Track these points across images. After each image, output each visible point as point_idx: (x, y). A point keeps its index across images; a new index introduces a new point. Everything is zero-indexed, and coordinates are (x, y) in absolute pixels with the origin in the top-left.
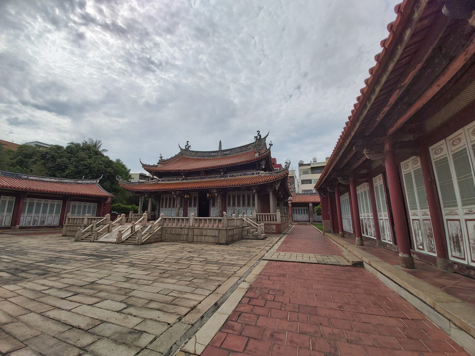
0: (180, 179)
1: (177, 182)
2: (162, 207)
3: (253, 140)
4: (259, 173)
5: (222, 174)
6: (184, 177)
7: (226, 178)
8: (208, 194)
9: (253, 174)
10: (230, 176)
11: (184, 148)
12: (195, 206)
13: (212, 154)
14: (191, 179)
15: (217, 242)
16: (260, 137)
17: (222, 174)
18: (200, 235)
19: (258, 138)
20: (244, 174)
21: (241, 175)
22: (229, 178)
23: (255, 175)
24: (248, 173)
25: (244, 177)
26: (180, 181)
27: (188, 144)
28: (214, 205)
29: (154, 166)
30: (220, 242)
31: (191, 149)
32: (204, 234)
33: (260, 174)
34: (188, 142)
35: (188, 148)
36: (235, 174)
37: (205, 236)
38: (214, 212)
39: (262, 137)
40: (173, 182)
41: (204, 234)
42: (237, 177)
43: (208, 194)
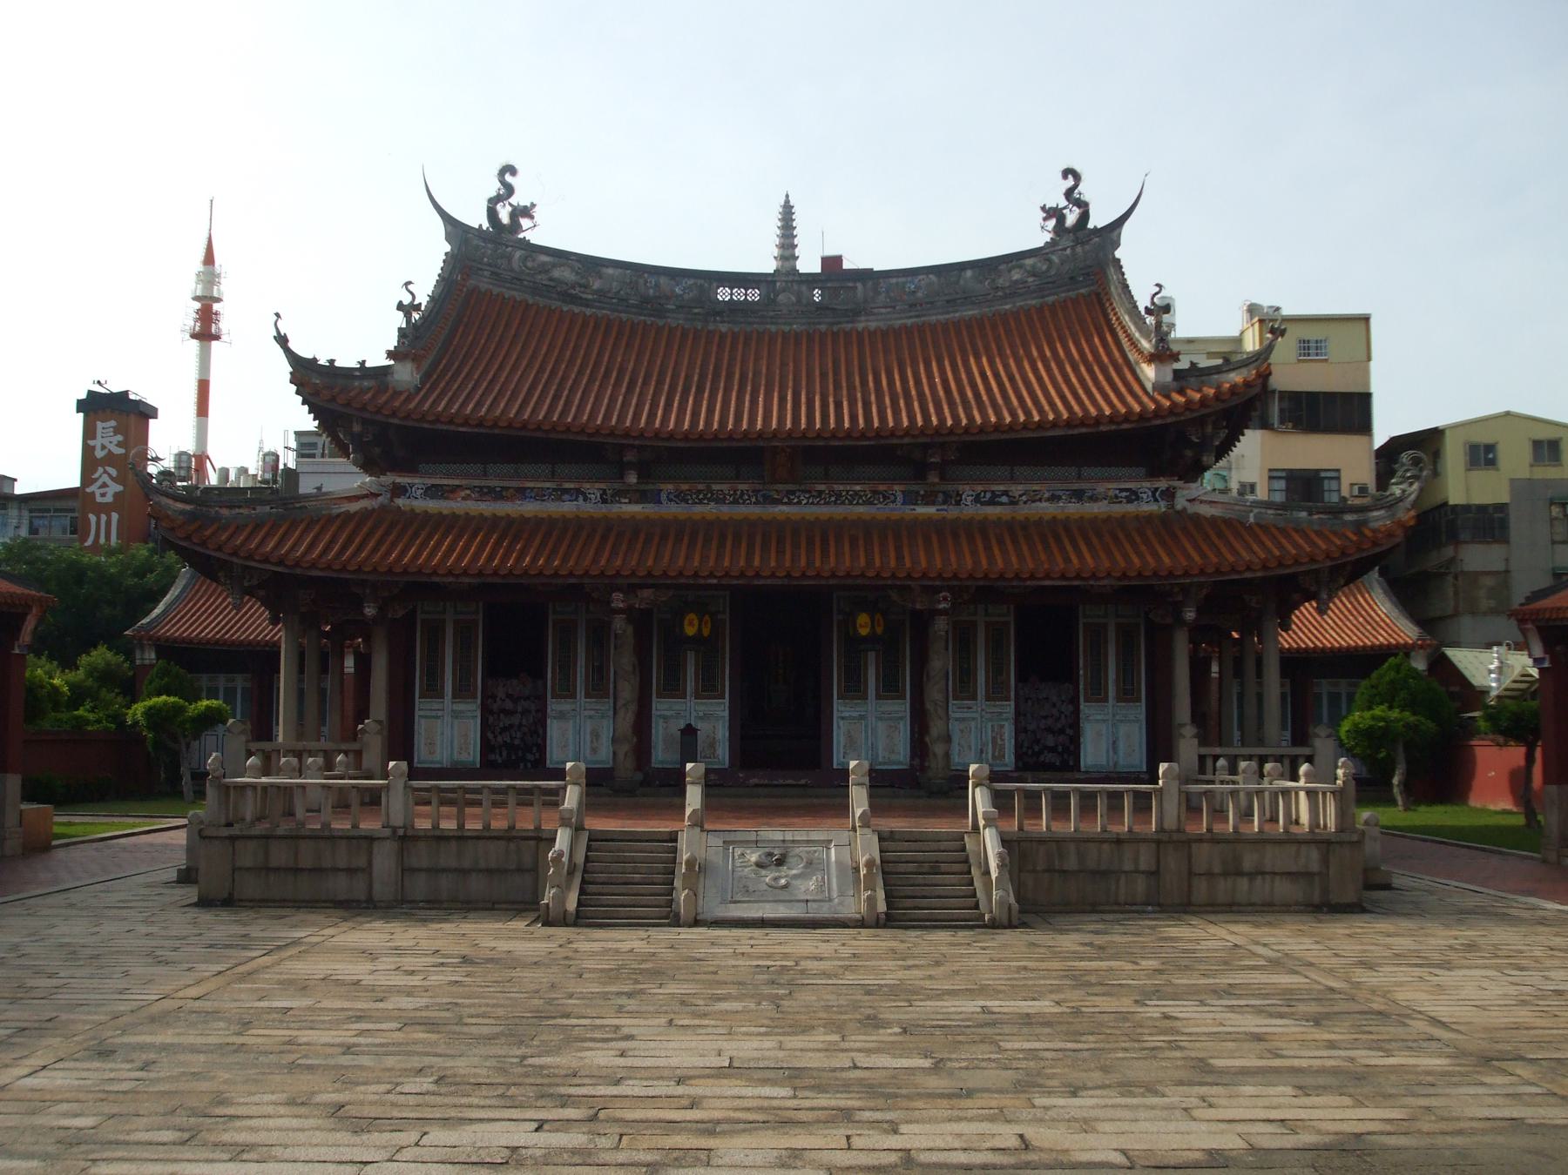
0: (593, 489)
1: (567, 507)
2: (433, 689)
3: (1034, 235)
4: (1169, 494)
5: (933, 478)
6: (632, 478)
7: (952, 512)
8: (863, 619)
9: (1134, 496)
10: (977, 500)
11: (477, 218)
12: (708, 688)
13: (723, 294)
14: (681, 497)
15: (1316, 899)
16: (1085, 217)
17: (933, 478)
18: (1225, 874)
19: (1071, 218)
20: (1078, 495)
21: (1054, 498)
22: (970, 510)
23: (1148, 507)
24: (1101, 488)
25: (1073, 509)
26: (589, 508)
27: (509, 190)
28: (854, 689)
29: (363, 371)
30: (1334, 898)
31: (538, 233)
32: (1248, 863)
33: (1180, 503)
34: (509, 169)
35: (515, 226)
36: (1017, 490)
37: (1252, 875)
38: (866, 733)
39: (1097, 220)
40: (529, 508)
41: (1248, 863)
42: (1025, 511)
43: (863, 619)
